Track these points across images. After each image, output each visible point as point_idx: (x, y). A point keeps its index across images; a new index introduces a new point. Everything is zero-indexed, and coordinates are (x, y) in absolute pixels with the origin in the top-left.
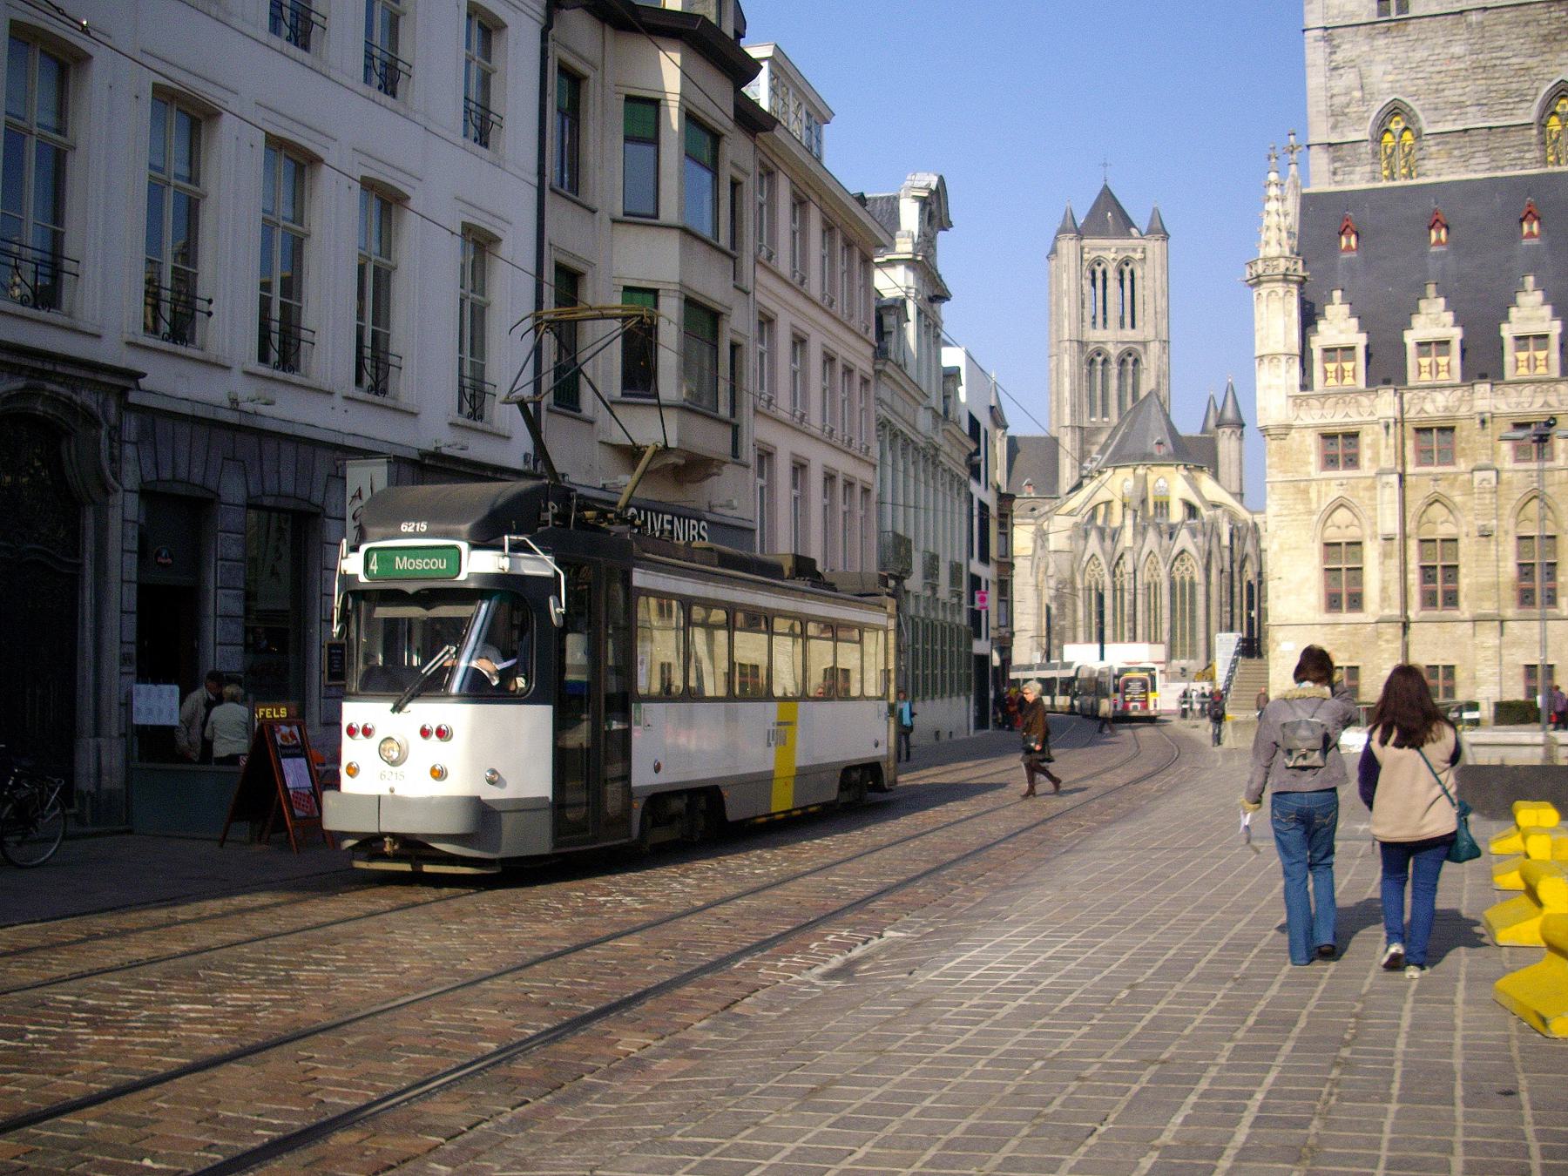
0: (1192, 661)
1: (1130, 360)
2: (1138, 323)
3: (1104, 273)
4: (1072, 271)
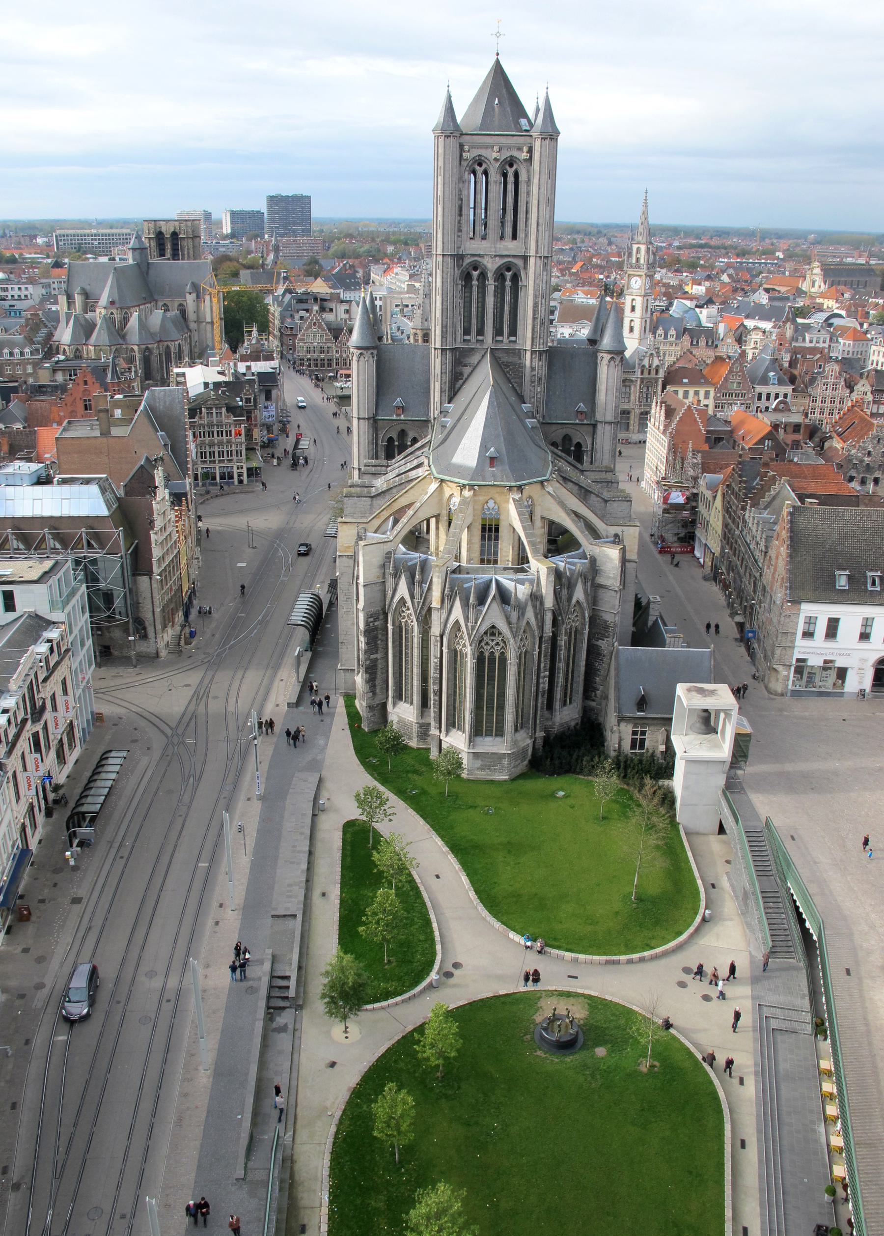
0: (499, 739)
1: (508, 275)
2: (521, 234)
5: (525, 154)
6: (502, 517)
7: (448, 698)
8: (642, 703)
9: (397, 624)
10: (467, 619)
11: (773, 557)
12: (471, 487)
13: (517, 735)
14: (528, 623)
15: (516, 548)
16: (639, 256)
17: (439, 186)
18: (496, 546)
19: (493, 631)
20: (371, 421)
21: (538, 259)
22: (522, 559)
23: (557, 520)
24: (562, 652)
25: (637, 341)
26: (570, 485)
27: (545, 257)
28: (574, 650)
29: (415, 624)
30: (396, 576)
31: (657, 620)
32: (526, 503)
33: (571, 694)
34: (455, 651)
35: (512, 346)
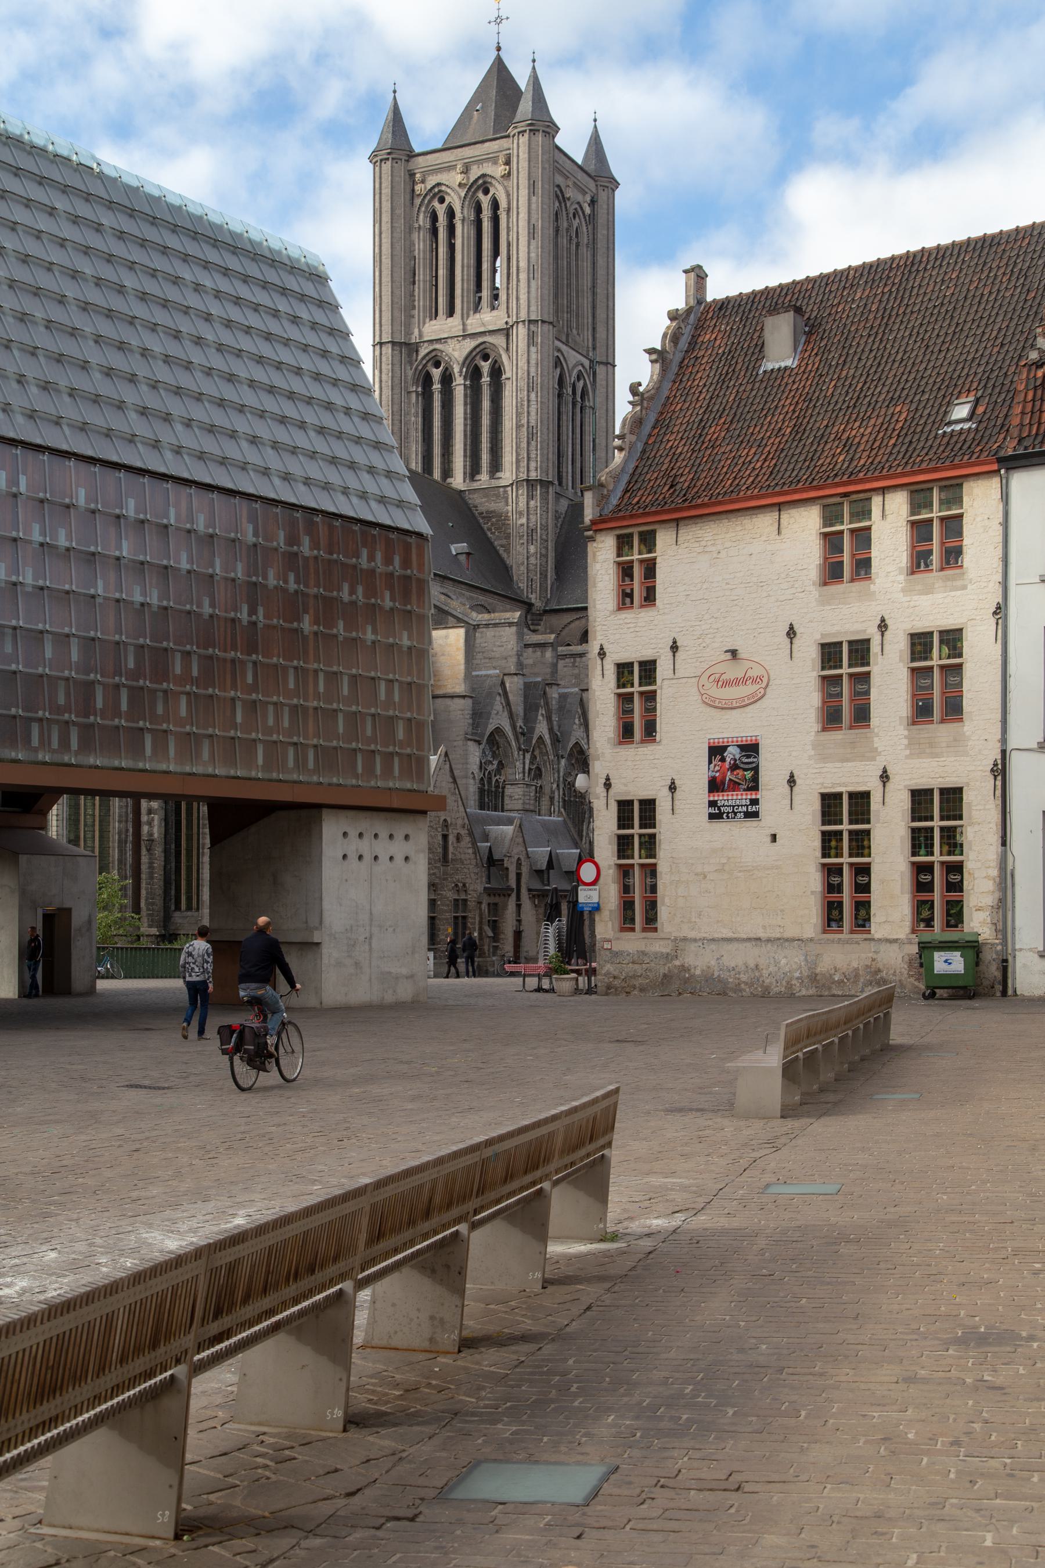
1: (485, 367)
3: (451, 214)
5: (503, 167)
21: (520, 325)
27: (530, 321)
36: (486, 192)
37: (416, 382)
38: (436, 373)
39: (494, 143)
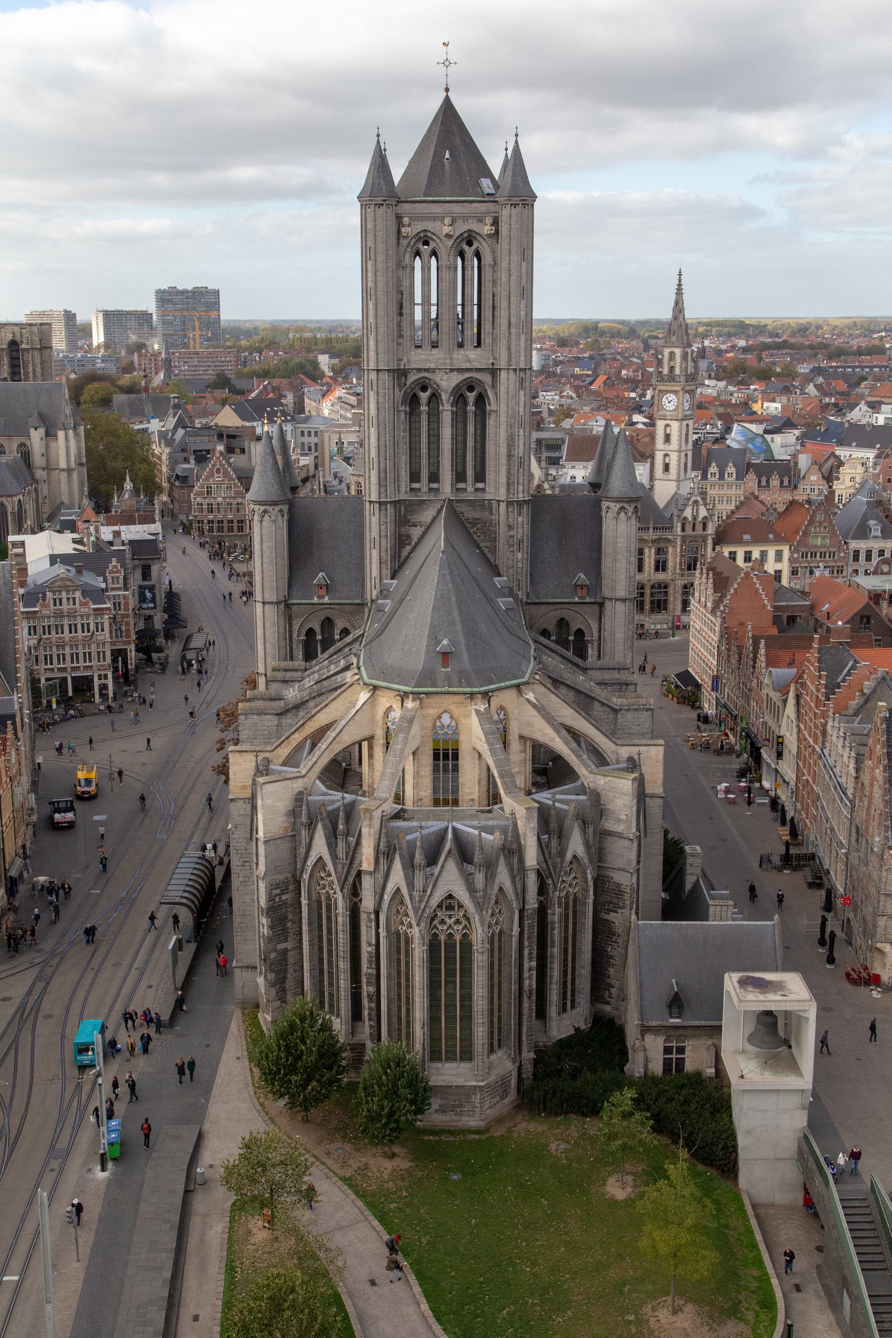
0: (466, 1065)
1: (471, 397)
2: (487, 339)
4: (380, 259)
5: (488, 227)
6: (462, 738)
7: (389, 1004)
8: (676, 1003)
9: (314, 897)
10: (411, 886)
11: (867, 783)
12: (416, 695)
13: (493, 1057)
14: (501, 889)
15: (484, 783)
16: (672, 364)
17: (370, 274)
18: (456, 780)
19: (450, 903)
20: (282, 606)
21: (512, 373)
22: (494, 798)
23: (542, 739)
24: (556, 931)
25: (675, 484)
26: (564, 690)
27: (520, 369)
28: (574, 929)
29: (339, 896)
30: (311, 826)
31: (698, 880)
32: (496, 717)
33: (573, 995)
34: (398, 934)
35: (480, 496)
36: (470, 244)
37: (403, 403)
38: (424, 396)
39: (481, 204)
